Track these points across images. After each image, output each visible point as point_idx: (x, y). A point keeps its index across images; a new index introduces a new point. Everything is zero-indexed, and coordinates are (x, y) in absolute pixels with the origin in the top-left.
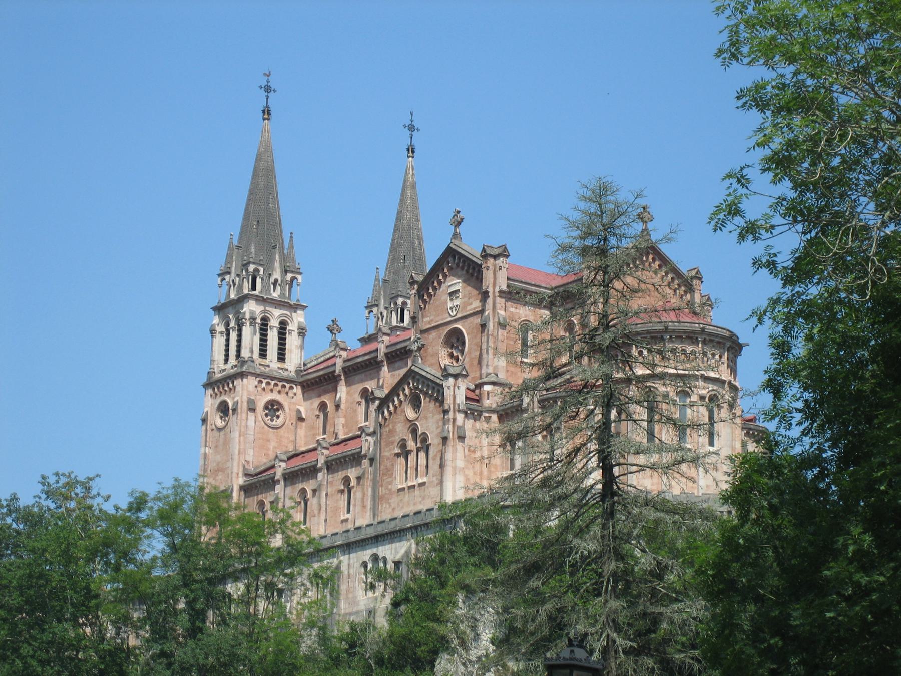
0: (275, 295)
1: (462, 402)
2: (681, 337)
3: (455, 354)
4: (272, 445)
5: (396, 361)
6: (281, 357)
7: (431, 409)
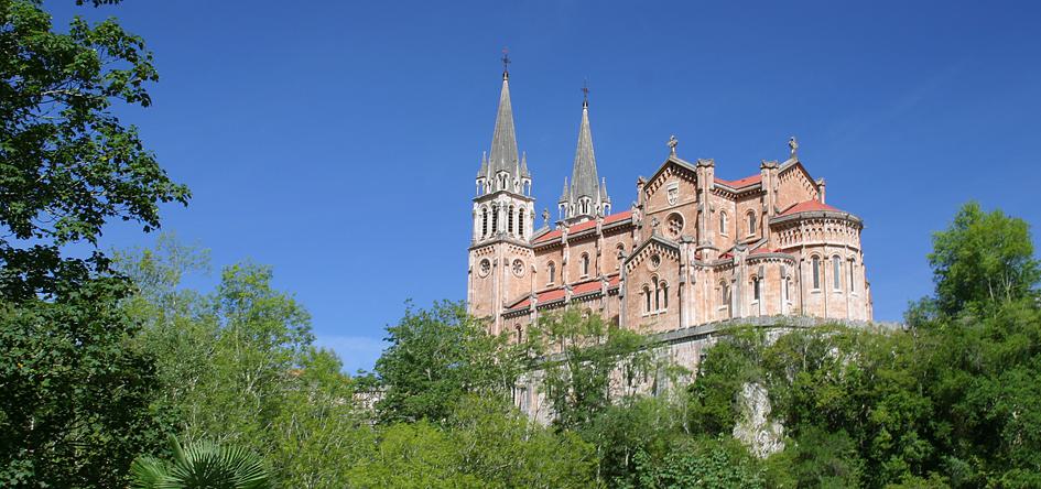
0: (517, 191)
6: (521, 233)
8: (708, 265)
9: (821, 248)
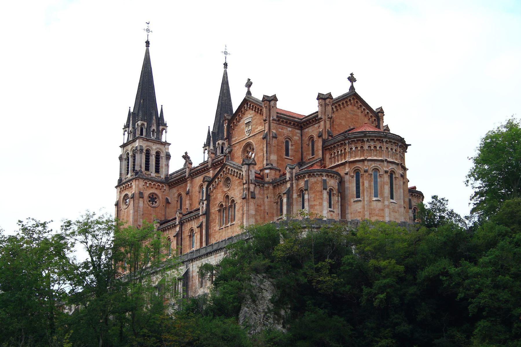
1: (253, 179)
2: (373, 140)
6: (157, 171)
7: (236, 184)
8: (268, 183)
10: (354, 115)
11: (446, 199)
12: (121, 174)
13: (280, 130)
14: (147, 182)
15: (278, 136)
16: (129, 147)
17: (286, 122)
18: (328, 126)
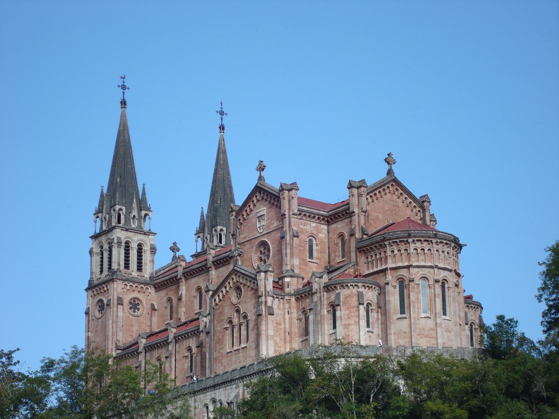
1: (271, 290)
2: (420, 241)
3: (263, 258)
4: (135, 328)
5: (220, 267)
6: (140, 269)
8: (290, 295)
9: (406, 270)
10: (394, 206)
11: (515, 320)
12: (92, 273)
13: (302, 226)
14: (127, 284)
15: (299, 234)
16: (103, 239)
17: (309, 216)
18: (362, 222)
